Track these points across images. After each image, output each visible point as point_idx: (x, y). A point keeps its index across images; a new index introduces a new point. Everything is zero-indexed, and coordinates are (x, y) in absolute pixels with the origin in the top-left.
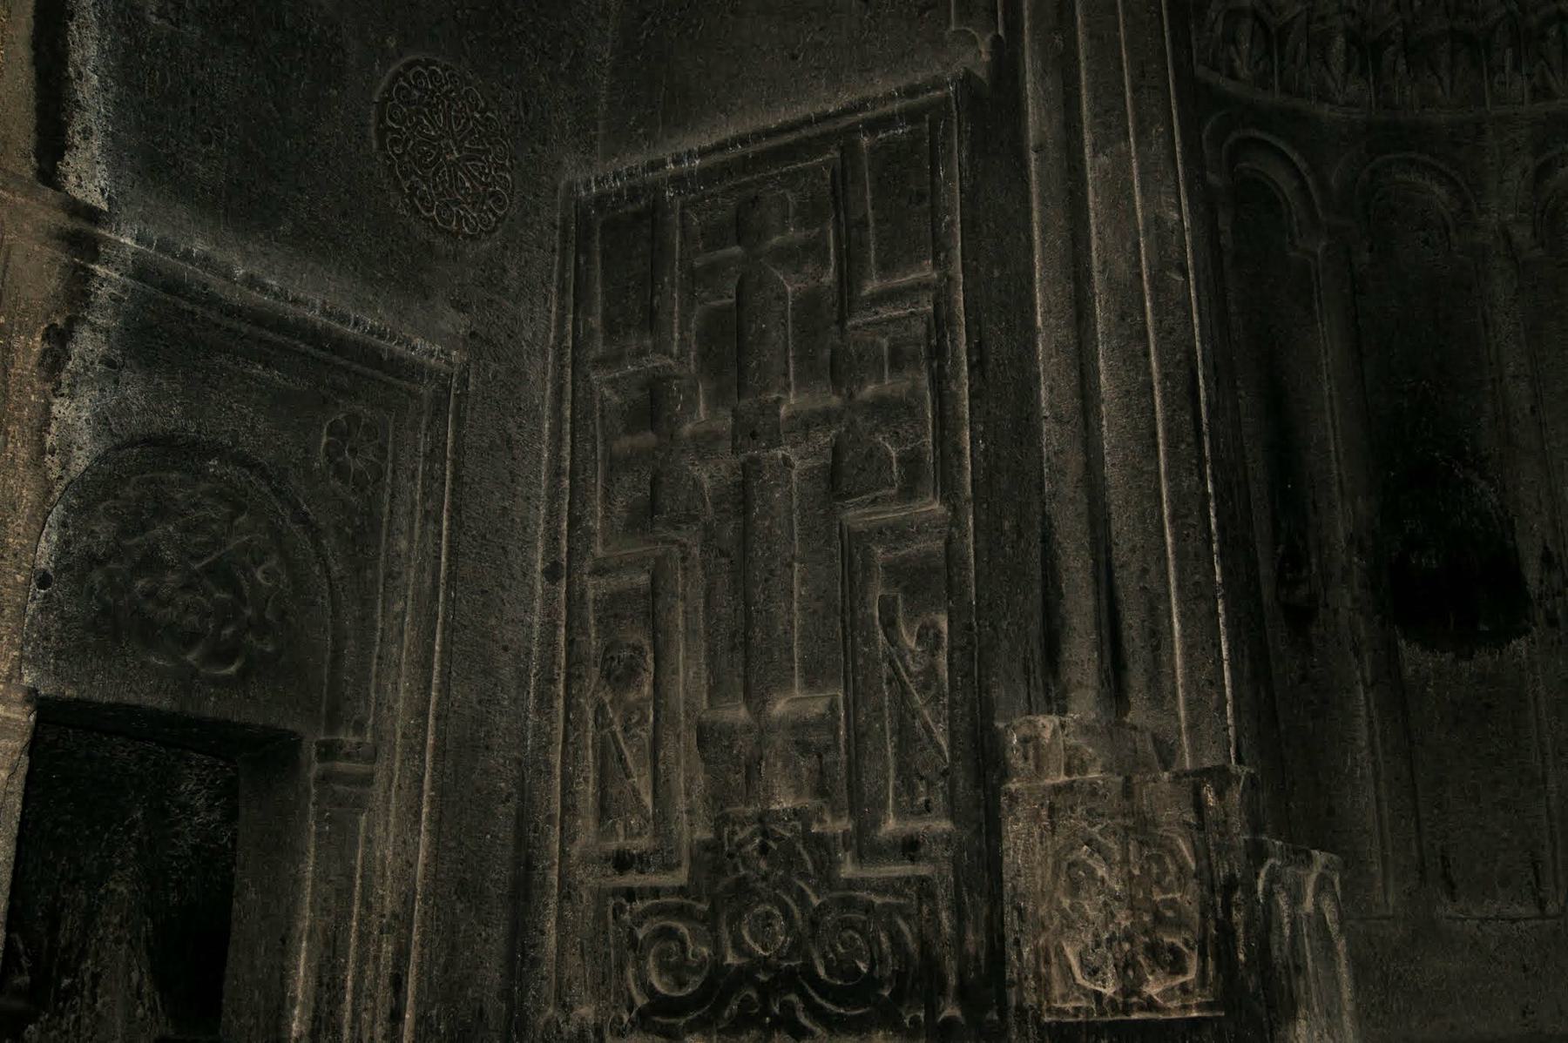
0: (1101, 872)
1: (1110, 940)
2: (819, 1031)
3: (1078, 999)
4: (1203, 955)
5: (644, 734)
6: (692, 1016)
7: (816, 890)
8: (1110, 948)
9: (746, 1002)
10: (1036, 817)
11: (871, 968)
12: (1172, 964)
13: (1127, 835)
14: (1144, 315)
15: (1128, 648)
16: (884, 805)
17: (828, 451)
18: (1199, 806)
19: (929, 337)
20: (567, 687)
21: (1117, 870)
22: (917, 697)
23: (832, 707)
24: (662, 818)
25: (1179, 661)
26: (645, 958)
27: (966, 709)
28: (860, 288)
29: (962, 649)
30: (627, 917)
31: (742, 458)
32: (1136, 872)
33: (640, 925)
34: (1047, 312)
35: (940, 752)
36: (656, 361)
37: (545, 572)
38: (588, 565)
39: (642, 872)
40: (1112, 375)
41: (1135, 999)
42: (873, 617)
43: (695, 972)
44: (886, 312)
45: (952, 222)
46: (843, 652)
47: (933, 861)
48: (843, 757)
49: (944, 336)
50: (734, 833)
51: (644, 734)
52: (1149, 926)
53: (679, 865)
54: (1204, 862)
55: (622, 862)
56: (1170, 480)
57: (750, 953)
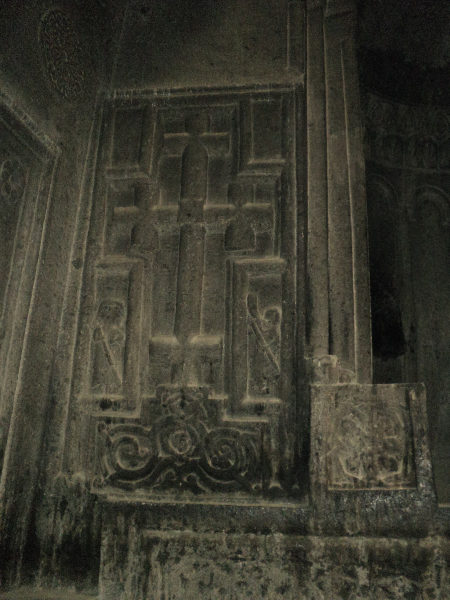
0: (358, 425)
1: (362, 455)
2: (207, 490)
3: (344, 480)
4: (406, 463)
5: (120, 345)
6: (139, 481)
7: (208, 425)
8: (362, 458)
9: (169, 476)
10: (328, 399)
11: (237, 463)
12: (391, 467)
13: (372, 409)
14: (349, 199)
15: (334, 334)
16: (244, 389)
17: (225, 228)
18: (408, 399)
19: (277, 186)
20: (81, 319)
21: (366, 425)
22: (265, 342)
23: (221, 343)
24: (128, 385)
25: (356, 342)
26: (115, 451)
27: (290, 349)
28: (247, 161)
29: (290, 323)
30: (105, 431)
31: (182, 224)
32: (376, 426)
33: (112, 435)
34: (312, 190)
35: (276, 368)
36: (141, 175)
37: (73, 262)
38: (97, 262)
39: (115, 410)
40: (333, 221)
41: (372, 481)
42: (245, 303)
43: (141, 459)
44: (257, 173)
45: (291, 142)
46: (228, 318)
47: (269, 416)
48: (223, 366)
49: (287, 187)
50: (167, 396)
51: (120, 345)
52: (382, 450)
53: (134, 409)
55: (105, 405)
56: (357, 267)
57: (172, 453)
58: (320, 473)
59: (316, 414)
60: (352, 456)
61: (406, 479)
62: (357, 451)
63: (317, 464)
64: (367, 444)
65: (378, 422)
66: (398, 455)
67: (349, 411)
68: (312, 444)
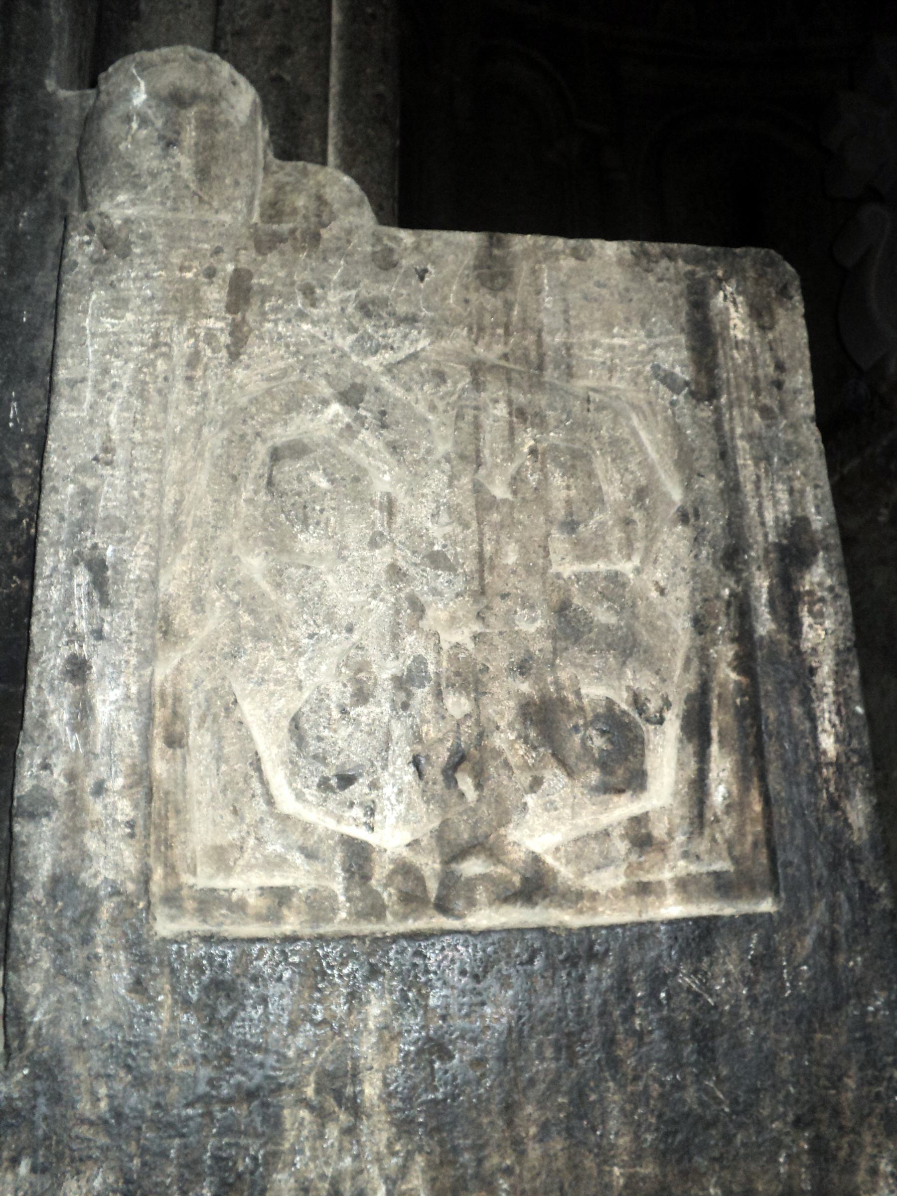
0: (384, 479)
1: (403, 683)
12: (604, 764)
18: (704, 338)
21: (437, 480)
32: (500, 491)
41: (472, 867)
52: (541, 646)
54: (710, 483)
58: (96, 808)
59: (88, 395)
60: (338, 692)
61: (702, 846)
62: (373, 653)
63: (73, 741)
64: (436, 614)
65: (512, 468)
66: (645, 683)
67: (326, 391)
68: (48, 594)
